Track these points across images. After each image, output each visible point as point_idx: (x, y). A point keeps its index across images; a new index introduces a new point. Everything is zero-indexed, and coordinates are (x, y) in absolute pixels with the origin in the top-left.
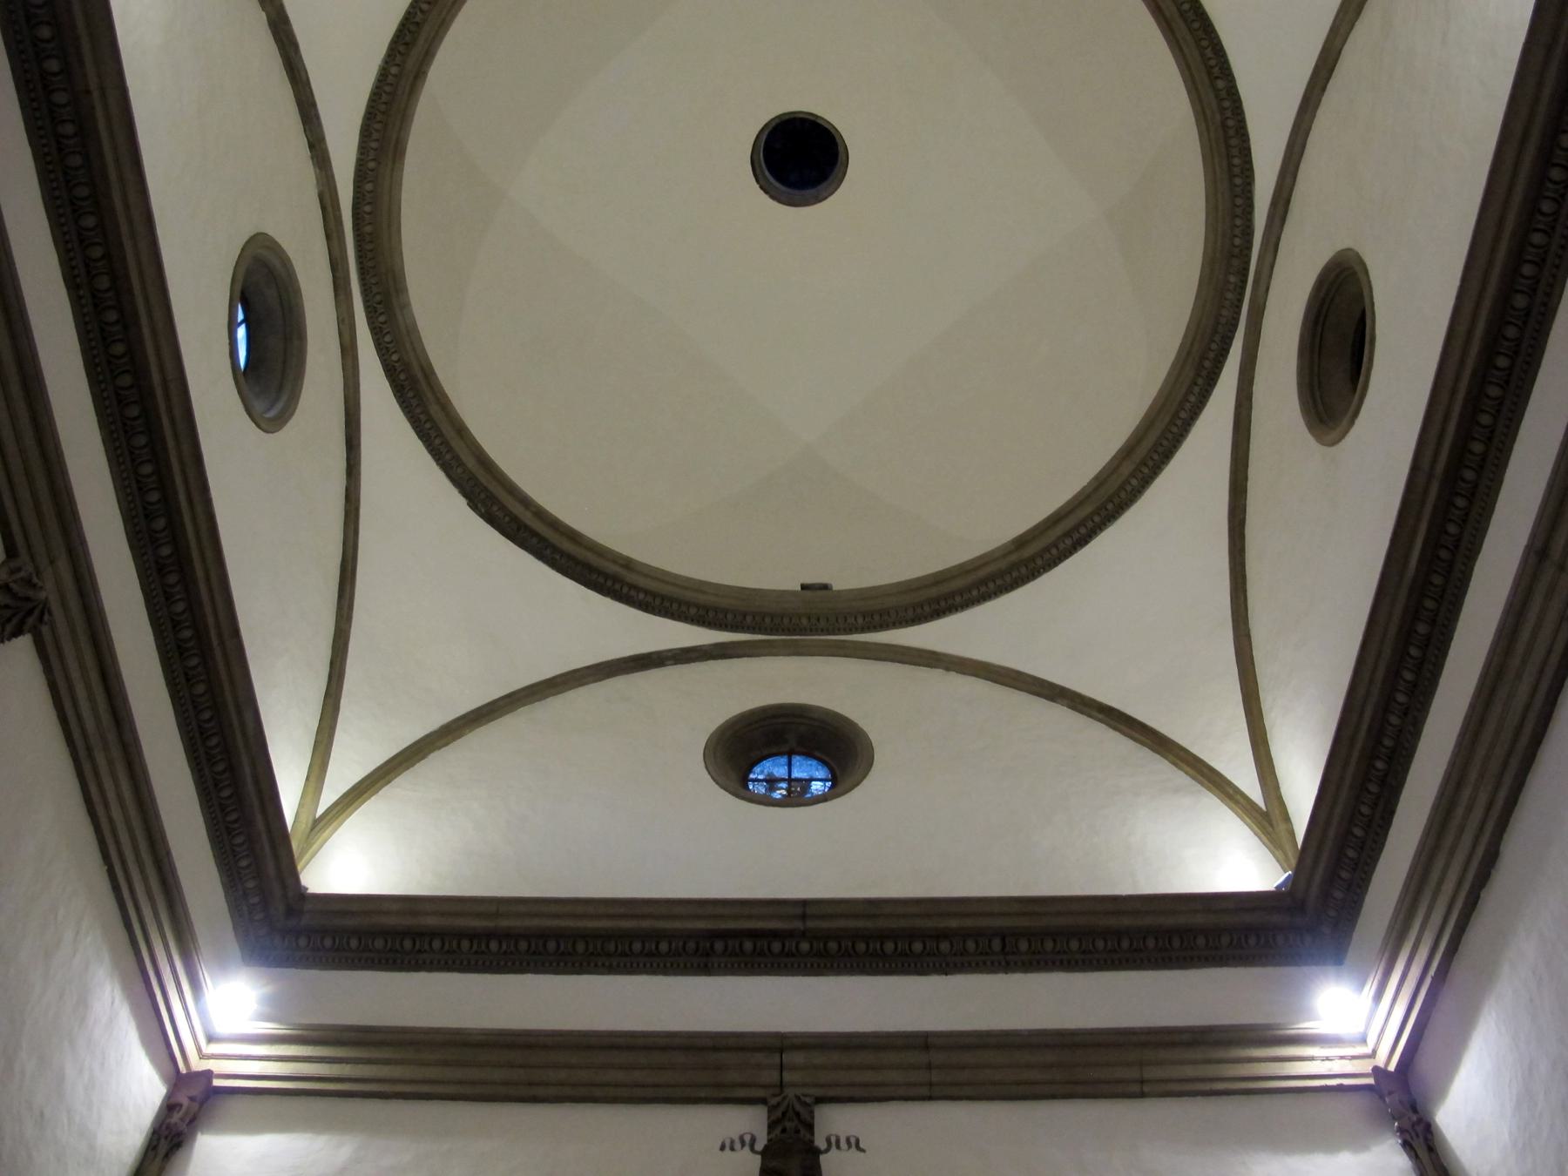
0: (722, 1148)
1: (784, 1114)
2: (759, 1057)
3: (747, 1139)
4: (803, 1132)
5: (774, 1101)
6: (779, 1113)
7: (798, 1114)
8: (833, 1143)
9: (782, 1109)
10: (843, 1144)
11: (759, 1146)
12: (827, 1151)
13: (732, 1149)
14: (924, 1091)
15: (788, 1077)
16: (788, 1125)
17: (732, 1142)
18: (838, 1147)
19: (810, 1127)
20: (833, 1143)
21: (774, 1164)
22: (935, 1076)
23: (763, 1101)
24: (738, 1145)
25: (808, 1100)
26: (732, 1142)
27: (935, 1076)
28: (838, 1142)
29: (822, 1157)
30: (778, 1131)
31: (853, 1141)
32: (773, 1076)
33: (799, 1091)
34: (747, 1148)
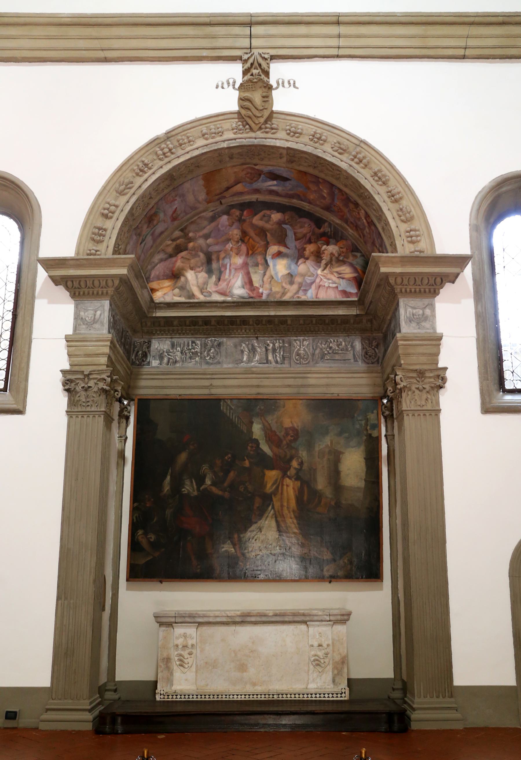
0: (217, 87)
1: (252, 64)
2: (237, 30)
3: (231, 81)
4: (263, 76)
5: (246, 57)
6: (248, 65)
7: (260, 65)
8: (280, 83)
9: (251, 61)
10: (286, 84)
11: (237, 86)
12: (277, 88)
13: (223, 88)
14: (334, 52)
15: (255, 42)
16: (255, 71)
17: (223, 84)
18: (283, 86)
19: (267, 74)
20: (280, 83)
21: (247, 94)
22: (343, 42)
23: (240, 58)
24: (225, 85)
25: (266, 56)
26: (223, 84)
27: (343, 42)
28: (283, 83)
29: (274, 92)
30: (248, 77)
31: (292, 82)
32: (245, 42)
33: (261, 51)
34: (231, 87)
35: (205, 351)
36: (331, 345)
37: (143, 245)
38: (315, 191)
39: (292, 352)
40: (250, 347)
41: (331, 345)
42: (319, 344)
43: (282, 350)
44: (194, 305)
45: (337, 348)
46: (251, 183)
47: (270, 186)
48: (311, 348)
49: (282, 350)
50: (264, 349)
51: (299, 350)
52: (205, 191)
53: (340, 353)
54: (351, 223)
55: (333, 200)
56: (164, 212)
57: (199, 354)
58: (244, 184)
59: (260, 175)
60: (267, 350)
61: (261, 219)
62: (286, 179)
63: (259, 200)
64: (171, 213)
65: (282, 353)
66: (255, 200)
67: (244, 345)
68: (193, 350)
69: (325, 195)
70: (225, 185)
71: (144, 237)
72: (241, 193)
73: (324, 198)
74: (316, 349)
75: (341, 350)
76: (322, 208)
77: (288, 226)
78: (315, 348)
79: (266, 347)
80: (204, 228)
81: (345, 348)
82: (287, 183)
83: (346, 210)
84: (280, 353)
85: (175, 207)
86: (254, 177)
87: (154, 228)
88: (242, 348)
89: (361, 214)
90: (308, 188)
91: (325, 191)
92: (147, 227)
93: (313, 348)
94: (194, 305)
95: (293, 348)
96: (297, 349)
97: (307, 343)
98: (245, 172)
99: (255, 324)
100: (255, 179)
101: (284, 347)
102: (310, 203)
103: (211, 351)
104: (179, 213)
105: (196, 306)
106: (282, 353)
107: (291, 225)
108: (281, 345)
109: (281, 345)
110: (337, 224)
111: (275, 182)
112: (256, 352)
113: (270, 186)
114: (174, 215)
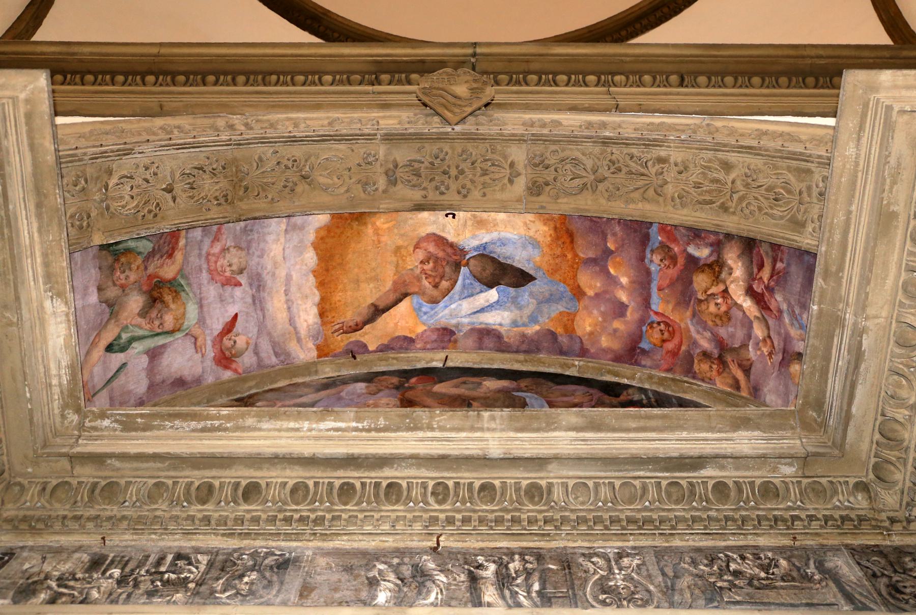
35: (218, 579)
36: (733, 566)
37: (117, 359)
38: (597, 295)
40: (407, 571)
41: (733, 566)
43: (536, 576)
44: (217, 423)
45: (763, 575)
46: (434, 301)
47: (482, 310)
49: (536, 576)
50: (463, 577)
52: (317, 299)
53: (782, 588)
54: (706, 355)
55: (646, 302)
56: (201, 307)
57: (192, 585)
58: (415, 299)
59: (457, 266)
60: (473, 579)
61: (456, 386)
62: (521, 278)
63: (450, 364)
64: (217, 326)
65: (536, 587)
66: (441, 365)
67: (381, 567)
68: (173, 576)
69: (623, 297)
70: (369, 294)
71: (125, 336)
72: (407, 342)
73: (620, 310)
75: (783, 580)
76: (618, 359)
77: (529, 394)
79: (470, 572)
80: (301, 396)
81: (795, 574)
82: (526, 294)
83: (684, 320)
85: (232, 311)
86: (442, 277)
87: (161, 341)
88: (374, 573)
89: (732, 288)
90: (578, 293)
91: (624, 280)
92: (143, 313)
94: (217, 423)
98: (421, 255)
99: (431, 500)
100: (445, 284)
102: (583, 353)
103: (246, 579)
104: (241, 342)
105: (226, 429)
107: (536, 393)
108: (529, 566)
110: (662, 381)
111: (493, 295)
112: (429, 584)
113: (482, 310)
114: (227, 342)
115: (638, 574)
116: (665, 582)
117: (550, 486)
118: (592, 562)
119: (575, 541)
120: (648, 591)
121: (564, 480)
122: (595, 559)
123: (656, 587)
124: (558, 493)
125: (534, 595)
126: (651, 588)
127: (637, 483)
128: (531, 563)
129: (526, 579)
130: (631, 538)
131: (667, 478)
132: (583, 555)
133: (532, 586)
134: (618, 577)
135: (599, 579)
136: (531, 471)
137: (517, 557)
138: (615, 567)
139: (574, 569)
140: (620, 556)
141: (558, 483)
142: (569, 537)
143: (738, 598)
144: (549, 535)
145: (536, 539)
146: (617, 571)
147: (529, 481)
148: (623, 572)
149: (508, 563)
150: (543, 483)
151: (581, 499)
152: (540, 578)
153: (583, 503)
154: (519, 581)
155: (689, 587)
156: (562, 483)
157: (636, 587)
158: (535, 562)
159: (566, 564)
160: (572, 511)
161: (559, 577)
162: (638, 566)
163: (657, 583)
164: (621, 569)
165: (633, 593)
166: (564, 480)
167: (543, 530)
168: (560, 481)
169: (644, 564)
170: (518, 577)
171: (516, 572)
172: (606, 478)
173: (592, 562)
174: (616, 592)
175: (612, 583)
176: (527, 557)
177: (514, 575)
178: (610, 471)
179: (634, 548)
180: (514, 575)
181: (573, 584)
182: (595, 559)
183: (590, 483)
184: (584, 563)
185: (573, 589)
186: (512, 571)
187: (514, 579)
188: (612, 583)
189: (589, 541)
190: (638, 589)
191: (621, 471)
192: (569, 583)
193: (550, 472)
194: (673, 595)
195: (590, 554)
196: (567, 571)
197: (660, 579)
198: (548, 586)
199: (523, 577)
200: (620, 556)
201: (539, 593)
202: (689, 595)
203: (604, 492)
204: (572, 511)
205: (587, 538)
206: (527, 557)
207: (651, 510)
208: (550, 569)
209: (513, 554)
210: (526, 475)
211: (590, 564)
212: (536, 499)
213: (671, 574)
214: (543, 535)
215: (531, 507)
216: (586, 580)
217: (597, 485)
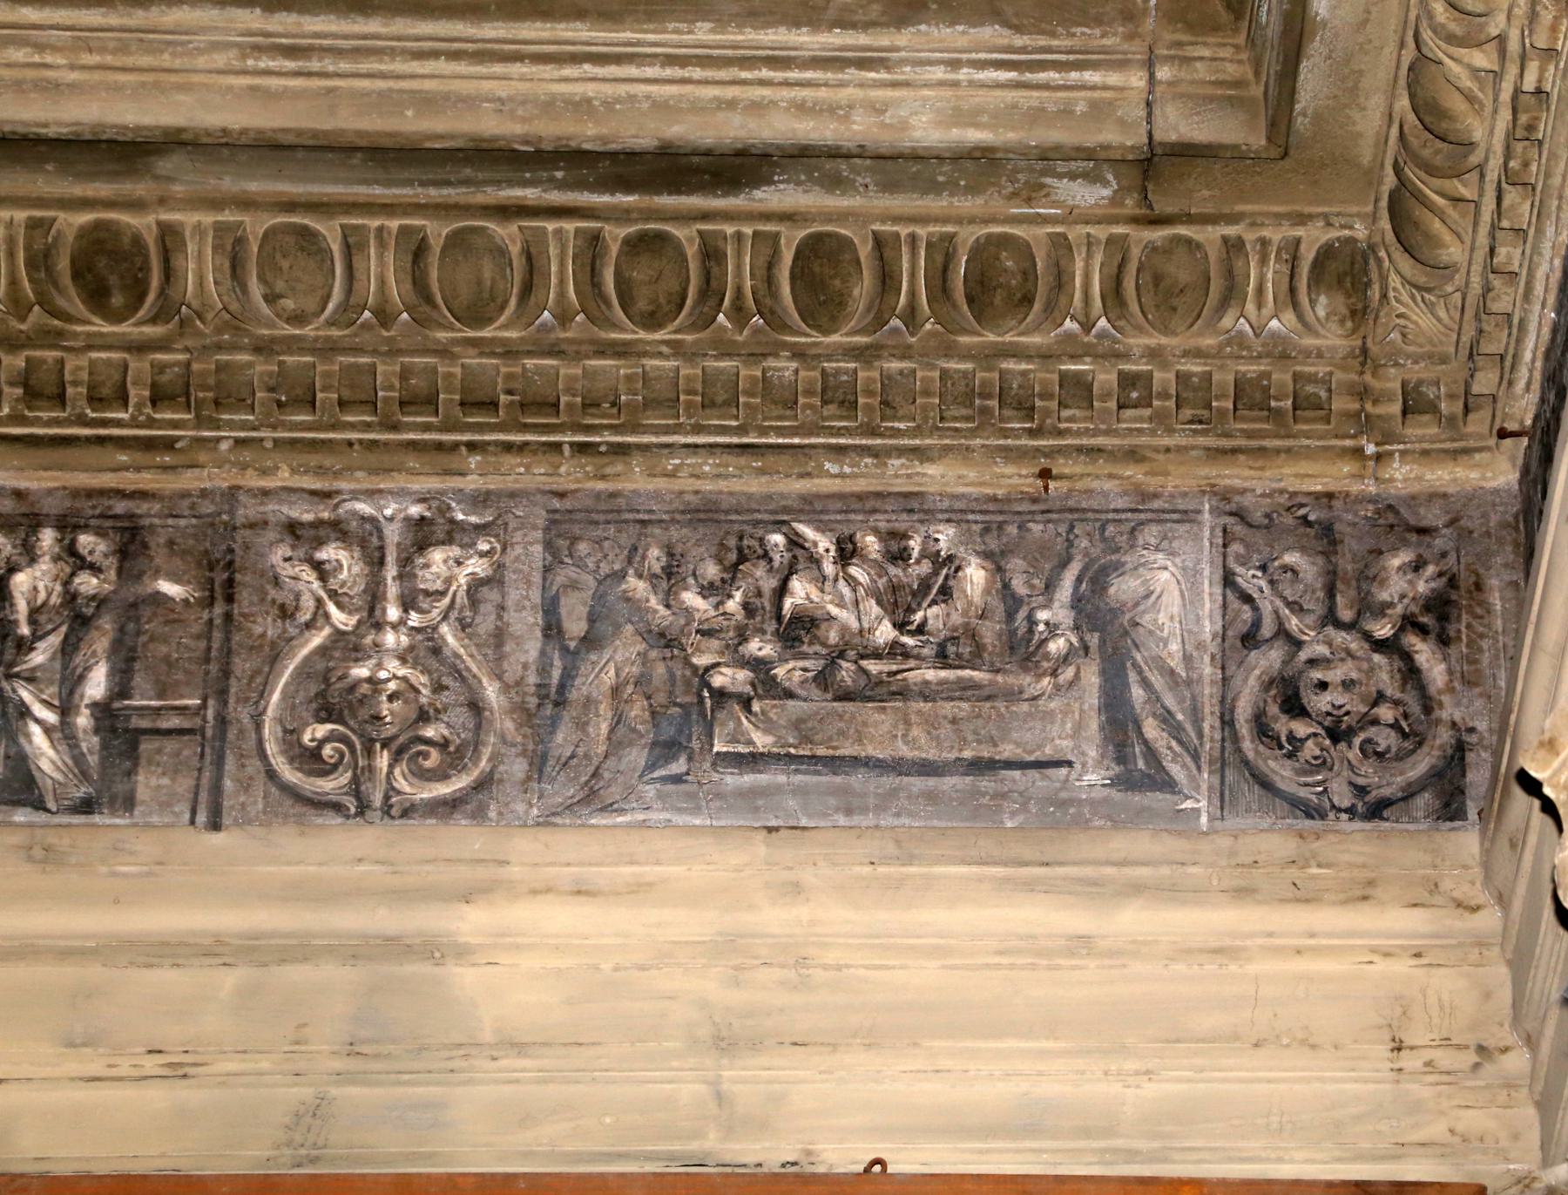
39: (242, 665)
42: (637, 586)
48: (525, 622)
51: (347, 646)
65: (97, 685)
74: (591, 641)
78: (575, 627)
84: (72, 682)
93: (552, 629)
95: (266, 626)
96: (317, 639)
97: (477, 566)
101: (137, 611)
106: (97, 685)
108: (87, 583)
109: (87, 583)
115: (464, 626)
116: (543, 670)
117: (169, 236)
118: (318, 566)
119: (264, 472)
120: (476, 707)
121: (228, 216)
122: (330, 553)
123: (506, 688)
124: (199, 271)
125: (83, 720)
126: (491, 692)
127: (508, 233)
128: (95, 569)
129: (68, 649)
130: (474, 460)
131: (622, 216)
132: (293, 529)
133: (81, 678)
134: (390, 639)
135: (322, 651)
136: (91, 176)
137: (47, 537)
138: (392, 590)
139: (245, 597)
140: (422, 535)
141: (199, 229)
142: (247, 455)
143: (762, 741)
144: (169, 445)
145: (123, 458)
146: (393, 613)
147: (85, 218)
148: (415, 619)
149: (12, 569)
150: (143, 223)
151: (289, 304)
152: (117, 646)
153: (298, 319)
154: (38, 657)
155: (616, 691)
156: (219, 228)
157: (438, 688)
158: (111, 564)
159: (220, 577)
160: (262, 348)
161: (184, 643)
162: (476, 584)
163: (512, 670)
164: (407, 604)
165: (423, 717)
166: (228, 216)
167: (151, 423)
168: (208, 218)
169: (495, 580)
170: (37, 637)
171: (34, 613)
172: (388, 209)
173: (318, 566)
174: (364, 713)
175: (361, 671)
176: (85, 540)
177: (25, 630)
178: (409, 183)
179: (480, 500)
180: (25, 630)
181: (226, 673)
182: (330, 553)
183: (330, 231)
184: (286, 571)
185: (222, 694)
186: (22, 607)
187: (24, 646)
188: (361, 671)
189: (320, 471)
190: (446, 697)
191: (448, 183)
192: (214, 668)
193: (170, 179)
194: (554, 723)
195: (318, 524)
196: (219, 609)
197: (533, 648)
198: (139, 680)
199: (55, 640)
200: (422, 535)
201: (104, 712)
202: (604, 728)
203: (382, 272)
204: (262, 348)
205: (314, 460)
206: (85, 540)
207: (554, 351)
208: (159, 599)
209: (35, 522)
210: (79, 190)
211: (309, 575)
212: (117, 300)
213: (575, 627)
214: (149, 445)
215: (103, 327)
216: (275, 658)
217: (352, 246)
